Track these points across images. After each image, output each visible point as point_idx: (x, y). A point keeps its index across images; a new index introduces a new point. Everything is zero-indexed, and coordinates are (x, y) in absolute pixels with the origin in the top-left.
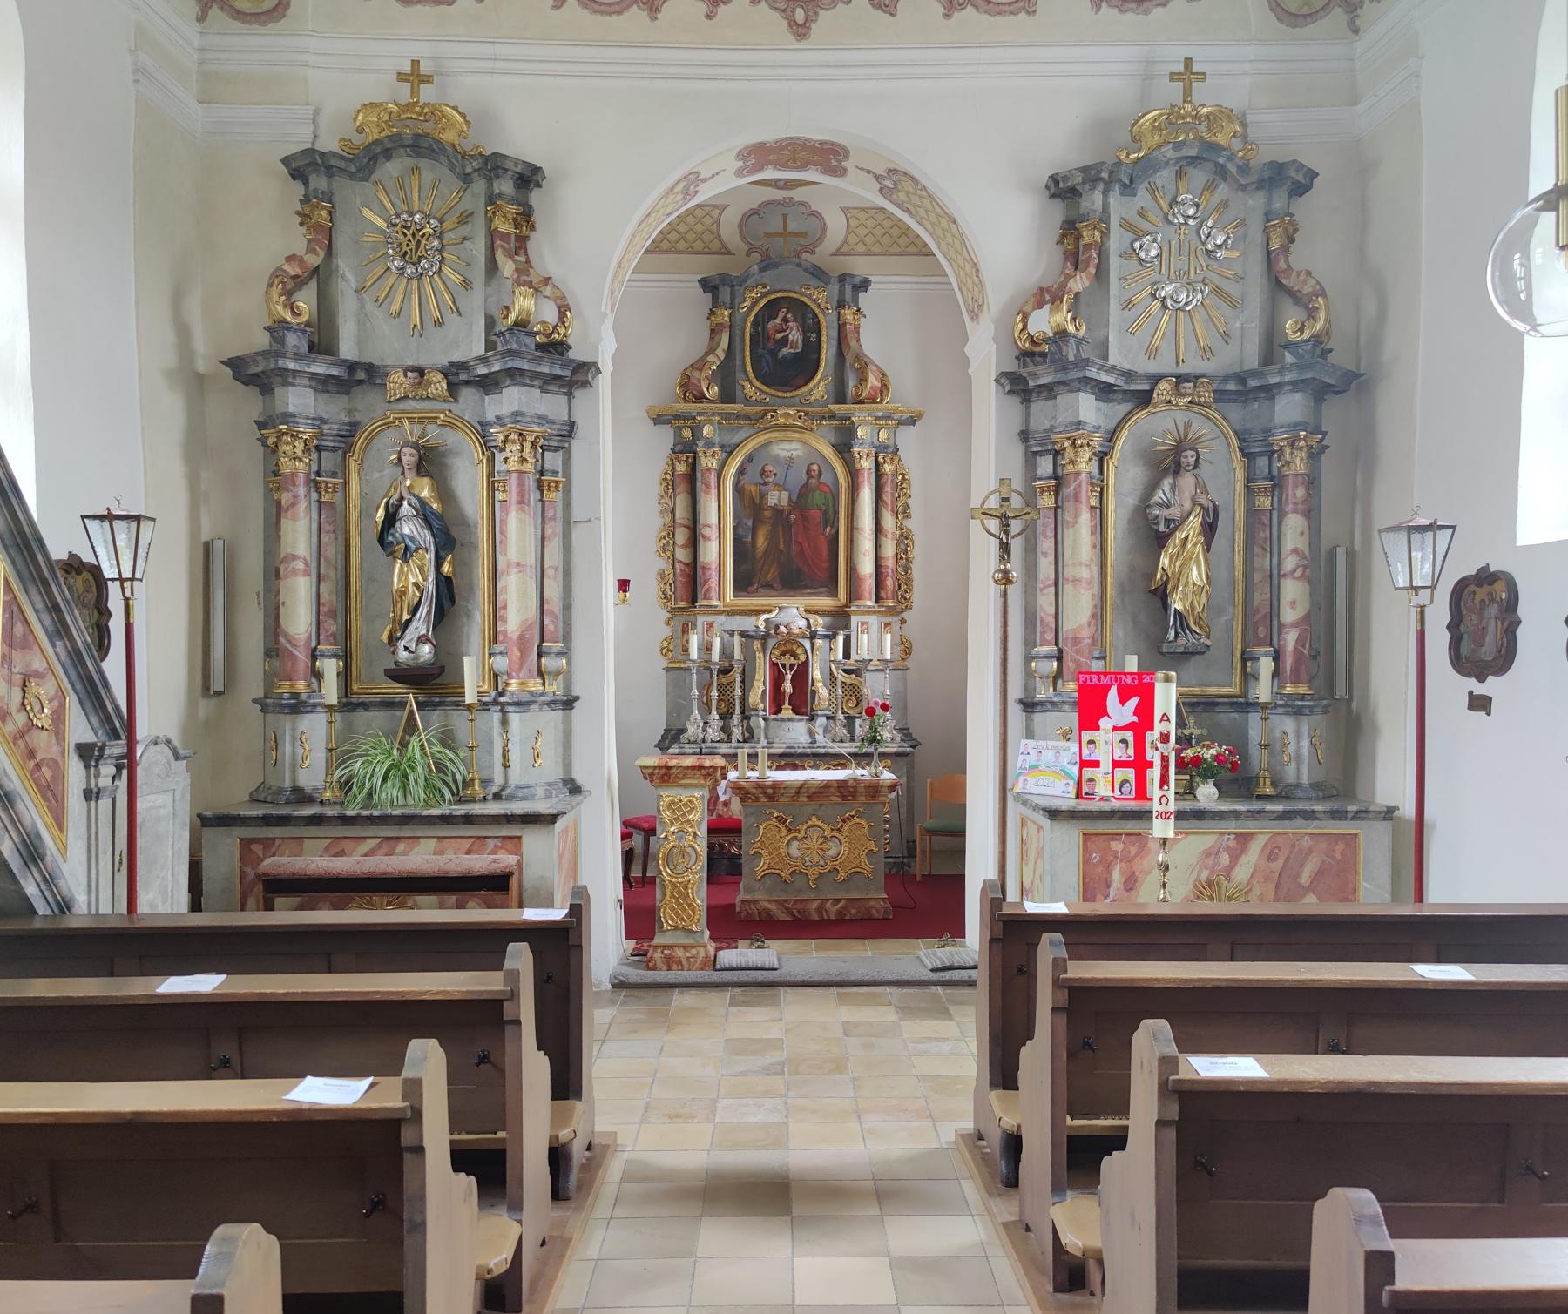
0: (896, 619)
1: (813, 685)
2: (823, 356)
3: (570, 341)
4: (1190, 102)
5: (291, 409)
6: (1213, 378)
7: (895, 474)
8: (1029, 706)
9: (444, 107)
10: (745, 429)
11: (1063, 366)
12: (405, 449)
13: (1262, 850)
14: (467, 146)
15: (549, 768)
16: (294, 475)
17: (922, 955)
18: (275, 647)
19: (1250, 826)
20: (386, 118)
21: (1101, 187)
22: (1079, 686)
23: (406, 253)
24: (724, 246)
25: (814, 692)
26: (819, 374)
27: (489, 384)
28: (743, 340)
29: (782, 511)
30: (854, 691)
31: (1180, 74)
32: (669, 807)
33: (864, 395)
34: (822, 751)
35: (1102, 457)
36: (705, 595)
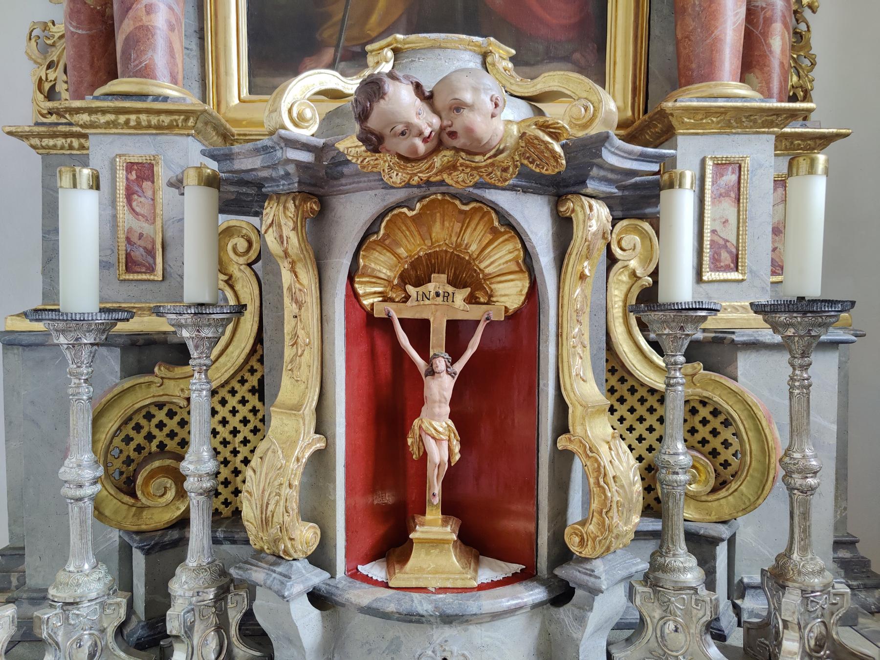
1: (562, 427)
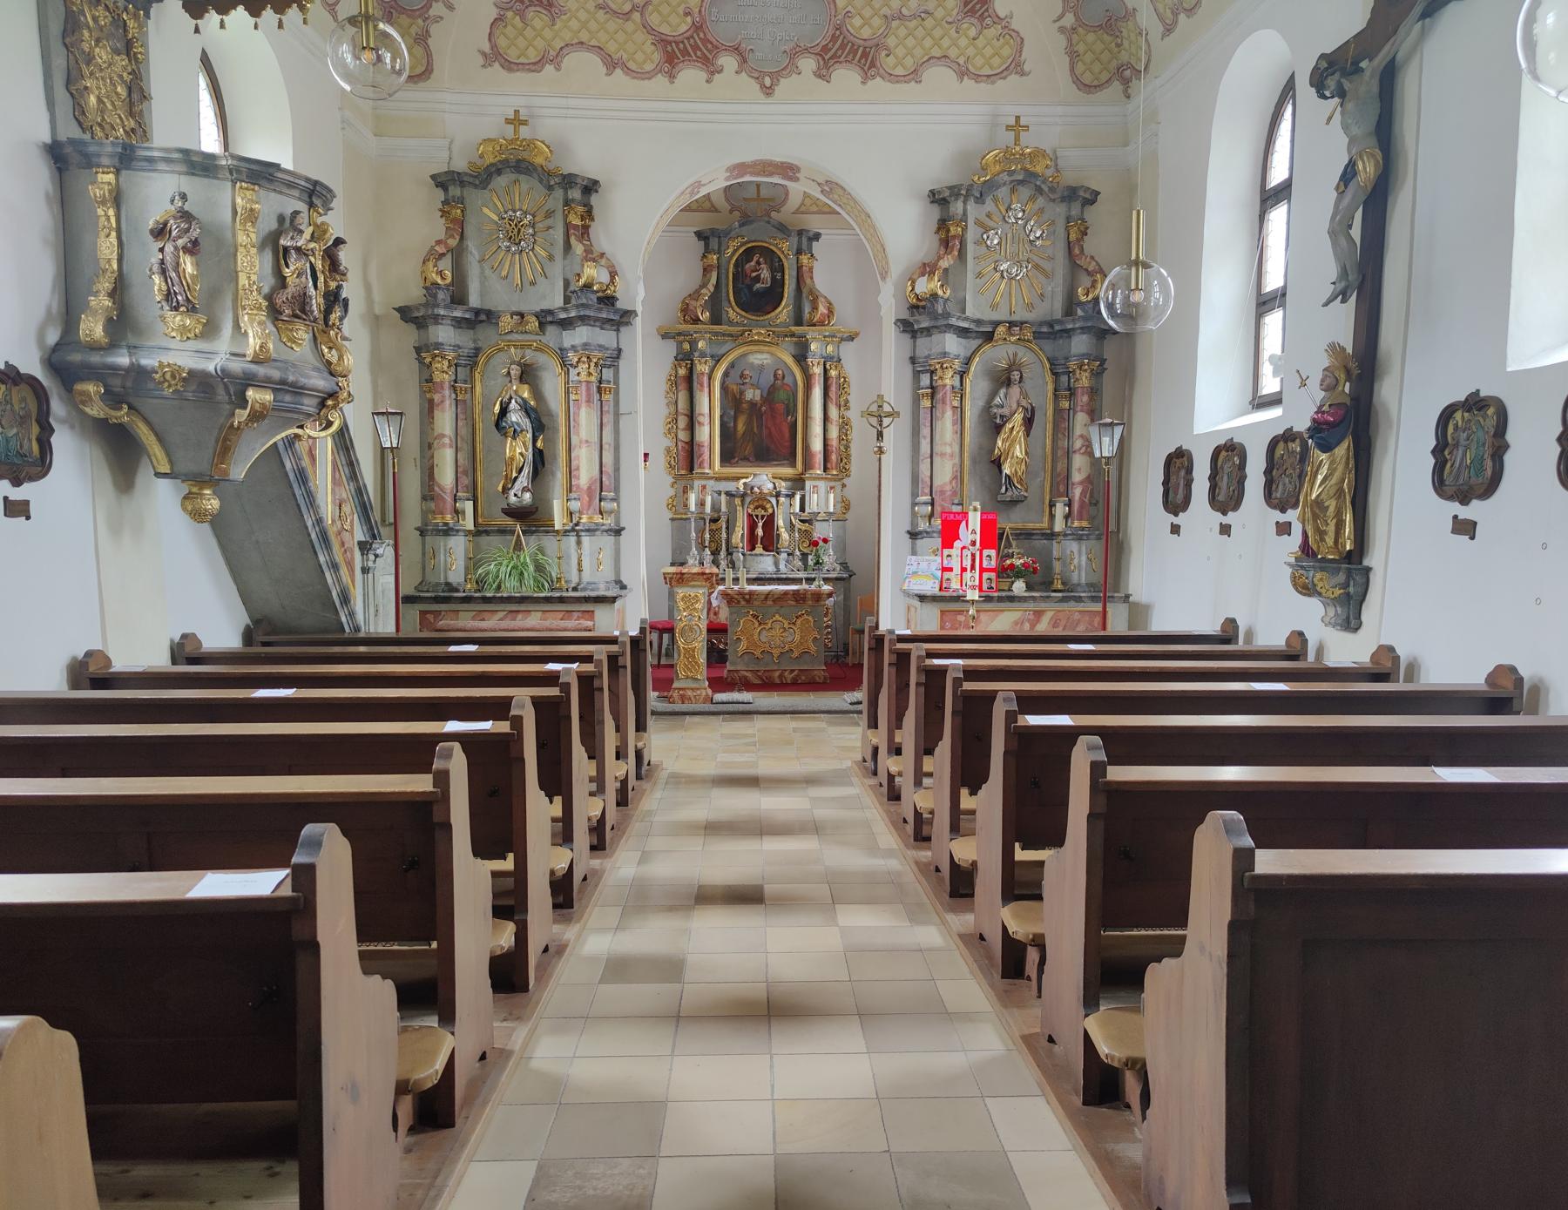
0: (838, 485)
1: (778, 530)
2: (786, 290)
3: (617, 295)
4: (1019, 145)
5: (440, 340)
6: (1032, 324)
7: (839, 377)
8: (914, 535)
9: (536, 142)
10: (729, 343)
11: (934, 316)
12: (513, 366)
13: (1050, 620)
14: (551, 167)
15: (607, 573)
16: (442, 383)
17: (848, 698)
18: (429, 491)
19: (1042, 606)
20: (499, 148)
21: (962, 198)
22: (942, 521)
23: (511, 237)
24: (713, 206)
25: (778, 535)
26: (783, 303)
27: (566, 324)
28: (727, 277)
29: (756, 404)
30: (806, 534)
31: (1013, 126)
32: (682, 600)
33: (815, 319)
34: (784, 576)
35: (962, 375)
36: (700, 465)
